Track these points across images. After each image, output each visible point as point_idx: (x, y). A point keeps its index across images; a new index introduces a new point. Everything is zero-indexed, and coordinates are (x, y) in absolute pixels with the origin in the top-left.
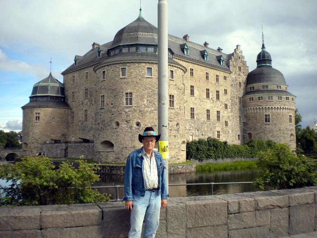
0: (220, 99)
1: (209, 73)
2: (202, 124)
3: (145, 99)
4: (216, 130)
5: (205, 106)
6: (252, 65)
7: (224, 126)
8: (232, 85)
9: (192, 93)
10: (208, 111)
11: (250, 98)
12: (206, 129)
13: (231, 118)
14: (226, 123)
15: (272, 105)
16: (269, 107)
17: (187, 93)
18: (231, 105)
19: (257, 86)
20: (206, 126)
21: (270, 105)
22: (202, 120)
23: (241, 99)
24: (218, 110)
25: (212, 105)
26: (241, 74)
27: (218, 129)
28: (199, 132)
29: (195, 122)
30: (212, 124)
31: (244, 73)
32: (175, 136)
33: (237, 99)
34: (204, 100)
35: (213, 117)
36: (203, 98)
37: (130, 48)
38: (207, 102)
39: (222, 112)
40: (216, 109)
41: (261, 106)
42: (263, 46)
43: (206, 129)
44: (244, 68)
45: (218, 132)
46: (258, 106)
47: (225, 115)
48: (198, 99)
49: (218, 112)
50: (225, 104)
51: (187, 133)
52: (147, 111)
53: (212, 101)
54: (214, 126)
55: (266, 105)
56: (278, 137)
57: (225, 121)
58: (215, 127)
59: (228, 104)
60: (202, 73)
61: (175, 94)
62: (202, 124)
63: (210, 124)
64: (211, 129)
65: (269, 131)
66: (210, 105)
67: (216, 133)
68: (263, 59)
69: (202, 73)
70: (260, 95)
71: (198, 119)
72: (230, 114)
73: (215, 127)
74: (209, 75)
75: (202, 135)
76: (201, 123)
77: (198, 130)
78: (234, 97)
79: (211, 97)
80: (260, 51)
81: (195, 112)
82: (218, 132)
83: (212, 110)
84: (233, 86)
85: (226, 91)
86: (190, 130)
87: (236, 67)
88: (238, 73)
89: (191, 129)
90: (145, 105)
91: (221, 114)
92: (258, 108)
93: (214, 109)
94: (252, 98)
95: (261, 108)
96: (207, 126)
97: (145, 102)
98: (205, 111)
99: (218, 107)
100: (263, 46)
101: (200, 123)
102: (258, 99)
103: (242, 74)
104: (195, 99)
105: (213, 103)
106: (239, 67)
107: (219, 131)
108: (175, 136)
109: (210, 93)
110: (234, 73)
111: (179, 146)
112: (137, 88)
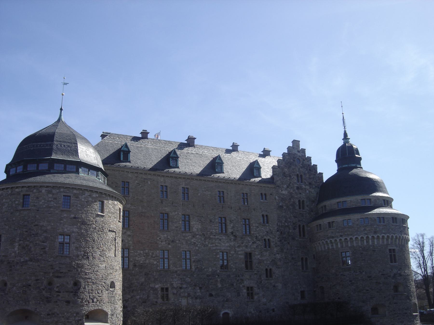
0: (252, 232)
1: (225, 191)
2: (210, 277)
3: (17, 244)
4: (244, 286)
5: (216, 246)
6: (328, 168)
7: (264, 277)
8: (282, 207)
9: (187, 227)
11: (317, 225)
12: (220, 285)
13: (279, 263)
14: (269, 273)
15: (351, 235)
16: (346, 239)
17: (174, 228)
18: (281, 241)
19: (332, 203)
20: (219, 280)
21: (348, 235)
22: (210, 270)
23: (306, 228)
24: (249, 250)
25: (232, 244)
26: (304, 186)
27: (246, 283)
28: (203, 290)
31: (310, 184)
32: (68, 302)
33: (294, 229)
34: (215, 236)
36: (211, 233)
37: (68, 166)
38: (220, 240)
39: (257, 253)
40: (242, 251)
41: (333, 237)
42: (345, 135)
43: (220, 285)
44: (312, 176)
45: (250, 289)
46: (328, 238)
47: (264, 258)
48: (200, 235)
49: (249, 256)
50: (265, 240)
51: (174, 294)
52: (17, 263)
53: (233, 237)
54: (238, 278)
55: (341, 236)
56: (368, 290)
57: (266, 270)
58: (242, 280)
59: (271, 239)
60: (210, 193)
61: (73, 232)
62: (210, 277)
64: (233, 285)
65: (351, 281)
67: (245, 291)
68: (347, 156)
69: (210, 193)
70: (330, 219)
72: (278, 256)
73: (242, 280)
74: (225, 194)
75: (211, 295)
76: (208, 276)
77: (201, 288)
78: (288, 226)
79: (230, 230)
80: (341, 143)
82: (250, 289)
84: (285, 207)
85: (266, 219)
86: (181, 288)
87: (290, 176)
88: (297, 185)
89: (184, 286)
90: (15, 252)
91: (257, 257)
92: (329, 242)
93: (237, 249)
94: (320, 225)
95: (333, 241)
97: (16, 249)
99: (246, 247)
100: (345, 135)
102: (327, 226)
103: (307, 187)
105: (235, 240)
106: (297, 175)
107: (252, 288)
108: (68, 302)
110: (285, 186)
111: (77, 318)
112: (7, 227)
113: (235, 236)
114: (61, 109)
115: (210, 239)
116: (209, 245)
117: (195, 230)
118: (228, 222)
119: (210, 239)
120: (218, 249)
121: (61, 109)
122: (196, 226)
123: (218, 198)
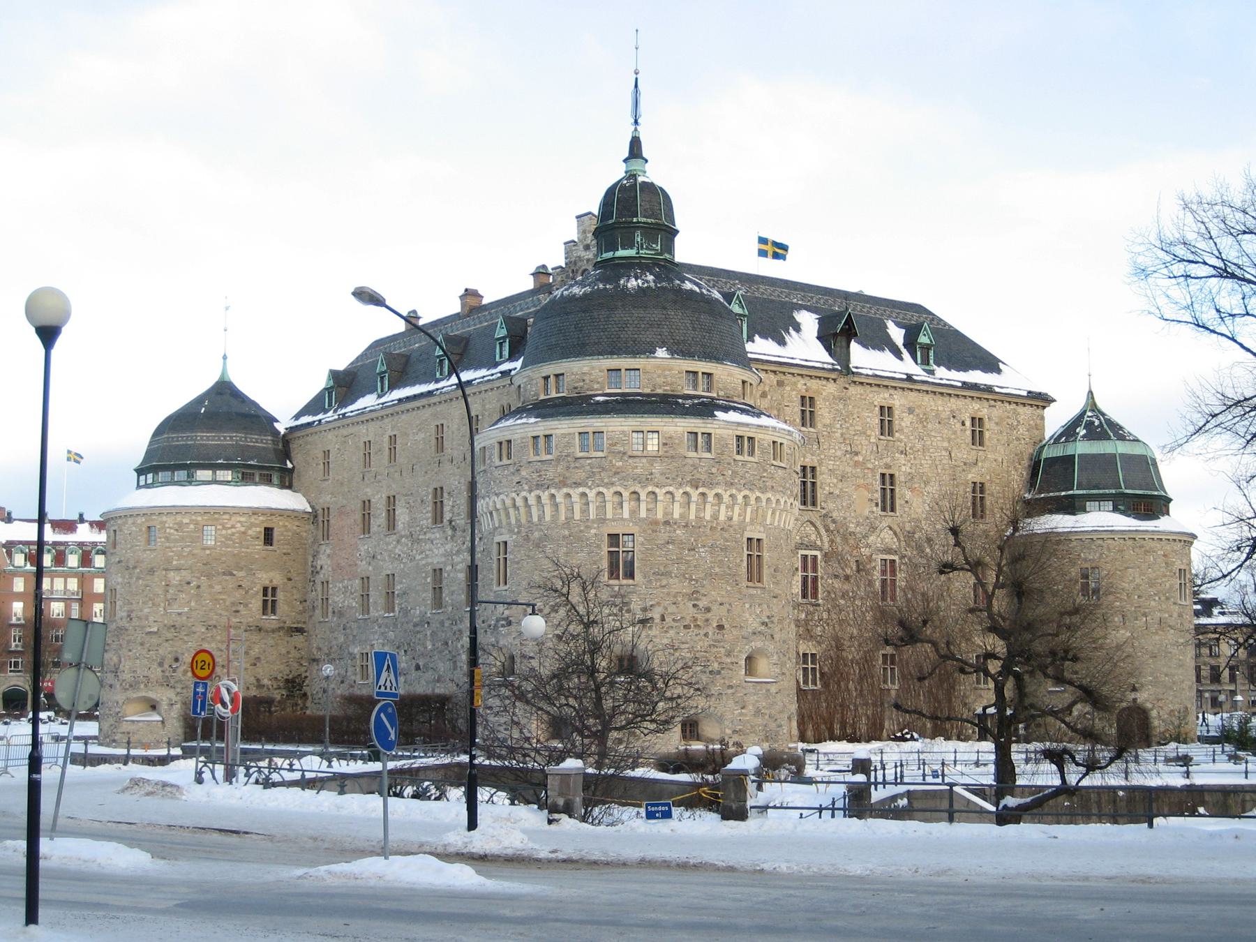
10: (438, 573)
25: (448, 547)
29: (395, 625)
30: (447, 624)
35: (452, 593)
53: (450, 532)
54: (455, 628)
60: (423, 435)
63: (442, 623)
66: (442, 551)
71: (406, 612)
75: (418, 668)
76: (416, 625)
79: (447, 516)
81: (398, 588)
83: (449, 568)
96: (433, 634)
98: (426, 578)
101: (411, 626)
104: (398, 542)
109: (445, 502)
113: (454, 529)
114: (225, 358)
115: (418, 541)
116: (418, 557)
117: (400, 526)
118: (445, 495)
119: (418, 541)
120: (428, 564)
121: (225, 358)
122: (402, 516)
123: (434, 441)
